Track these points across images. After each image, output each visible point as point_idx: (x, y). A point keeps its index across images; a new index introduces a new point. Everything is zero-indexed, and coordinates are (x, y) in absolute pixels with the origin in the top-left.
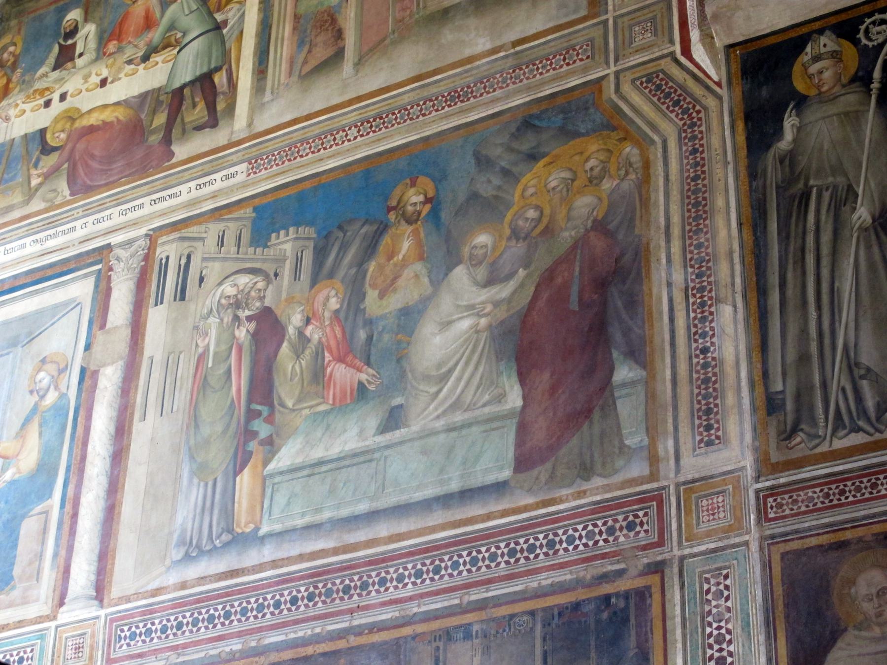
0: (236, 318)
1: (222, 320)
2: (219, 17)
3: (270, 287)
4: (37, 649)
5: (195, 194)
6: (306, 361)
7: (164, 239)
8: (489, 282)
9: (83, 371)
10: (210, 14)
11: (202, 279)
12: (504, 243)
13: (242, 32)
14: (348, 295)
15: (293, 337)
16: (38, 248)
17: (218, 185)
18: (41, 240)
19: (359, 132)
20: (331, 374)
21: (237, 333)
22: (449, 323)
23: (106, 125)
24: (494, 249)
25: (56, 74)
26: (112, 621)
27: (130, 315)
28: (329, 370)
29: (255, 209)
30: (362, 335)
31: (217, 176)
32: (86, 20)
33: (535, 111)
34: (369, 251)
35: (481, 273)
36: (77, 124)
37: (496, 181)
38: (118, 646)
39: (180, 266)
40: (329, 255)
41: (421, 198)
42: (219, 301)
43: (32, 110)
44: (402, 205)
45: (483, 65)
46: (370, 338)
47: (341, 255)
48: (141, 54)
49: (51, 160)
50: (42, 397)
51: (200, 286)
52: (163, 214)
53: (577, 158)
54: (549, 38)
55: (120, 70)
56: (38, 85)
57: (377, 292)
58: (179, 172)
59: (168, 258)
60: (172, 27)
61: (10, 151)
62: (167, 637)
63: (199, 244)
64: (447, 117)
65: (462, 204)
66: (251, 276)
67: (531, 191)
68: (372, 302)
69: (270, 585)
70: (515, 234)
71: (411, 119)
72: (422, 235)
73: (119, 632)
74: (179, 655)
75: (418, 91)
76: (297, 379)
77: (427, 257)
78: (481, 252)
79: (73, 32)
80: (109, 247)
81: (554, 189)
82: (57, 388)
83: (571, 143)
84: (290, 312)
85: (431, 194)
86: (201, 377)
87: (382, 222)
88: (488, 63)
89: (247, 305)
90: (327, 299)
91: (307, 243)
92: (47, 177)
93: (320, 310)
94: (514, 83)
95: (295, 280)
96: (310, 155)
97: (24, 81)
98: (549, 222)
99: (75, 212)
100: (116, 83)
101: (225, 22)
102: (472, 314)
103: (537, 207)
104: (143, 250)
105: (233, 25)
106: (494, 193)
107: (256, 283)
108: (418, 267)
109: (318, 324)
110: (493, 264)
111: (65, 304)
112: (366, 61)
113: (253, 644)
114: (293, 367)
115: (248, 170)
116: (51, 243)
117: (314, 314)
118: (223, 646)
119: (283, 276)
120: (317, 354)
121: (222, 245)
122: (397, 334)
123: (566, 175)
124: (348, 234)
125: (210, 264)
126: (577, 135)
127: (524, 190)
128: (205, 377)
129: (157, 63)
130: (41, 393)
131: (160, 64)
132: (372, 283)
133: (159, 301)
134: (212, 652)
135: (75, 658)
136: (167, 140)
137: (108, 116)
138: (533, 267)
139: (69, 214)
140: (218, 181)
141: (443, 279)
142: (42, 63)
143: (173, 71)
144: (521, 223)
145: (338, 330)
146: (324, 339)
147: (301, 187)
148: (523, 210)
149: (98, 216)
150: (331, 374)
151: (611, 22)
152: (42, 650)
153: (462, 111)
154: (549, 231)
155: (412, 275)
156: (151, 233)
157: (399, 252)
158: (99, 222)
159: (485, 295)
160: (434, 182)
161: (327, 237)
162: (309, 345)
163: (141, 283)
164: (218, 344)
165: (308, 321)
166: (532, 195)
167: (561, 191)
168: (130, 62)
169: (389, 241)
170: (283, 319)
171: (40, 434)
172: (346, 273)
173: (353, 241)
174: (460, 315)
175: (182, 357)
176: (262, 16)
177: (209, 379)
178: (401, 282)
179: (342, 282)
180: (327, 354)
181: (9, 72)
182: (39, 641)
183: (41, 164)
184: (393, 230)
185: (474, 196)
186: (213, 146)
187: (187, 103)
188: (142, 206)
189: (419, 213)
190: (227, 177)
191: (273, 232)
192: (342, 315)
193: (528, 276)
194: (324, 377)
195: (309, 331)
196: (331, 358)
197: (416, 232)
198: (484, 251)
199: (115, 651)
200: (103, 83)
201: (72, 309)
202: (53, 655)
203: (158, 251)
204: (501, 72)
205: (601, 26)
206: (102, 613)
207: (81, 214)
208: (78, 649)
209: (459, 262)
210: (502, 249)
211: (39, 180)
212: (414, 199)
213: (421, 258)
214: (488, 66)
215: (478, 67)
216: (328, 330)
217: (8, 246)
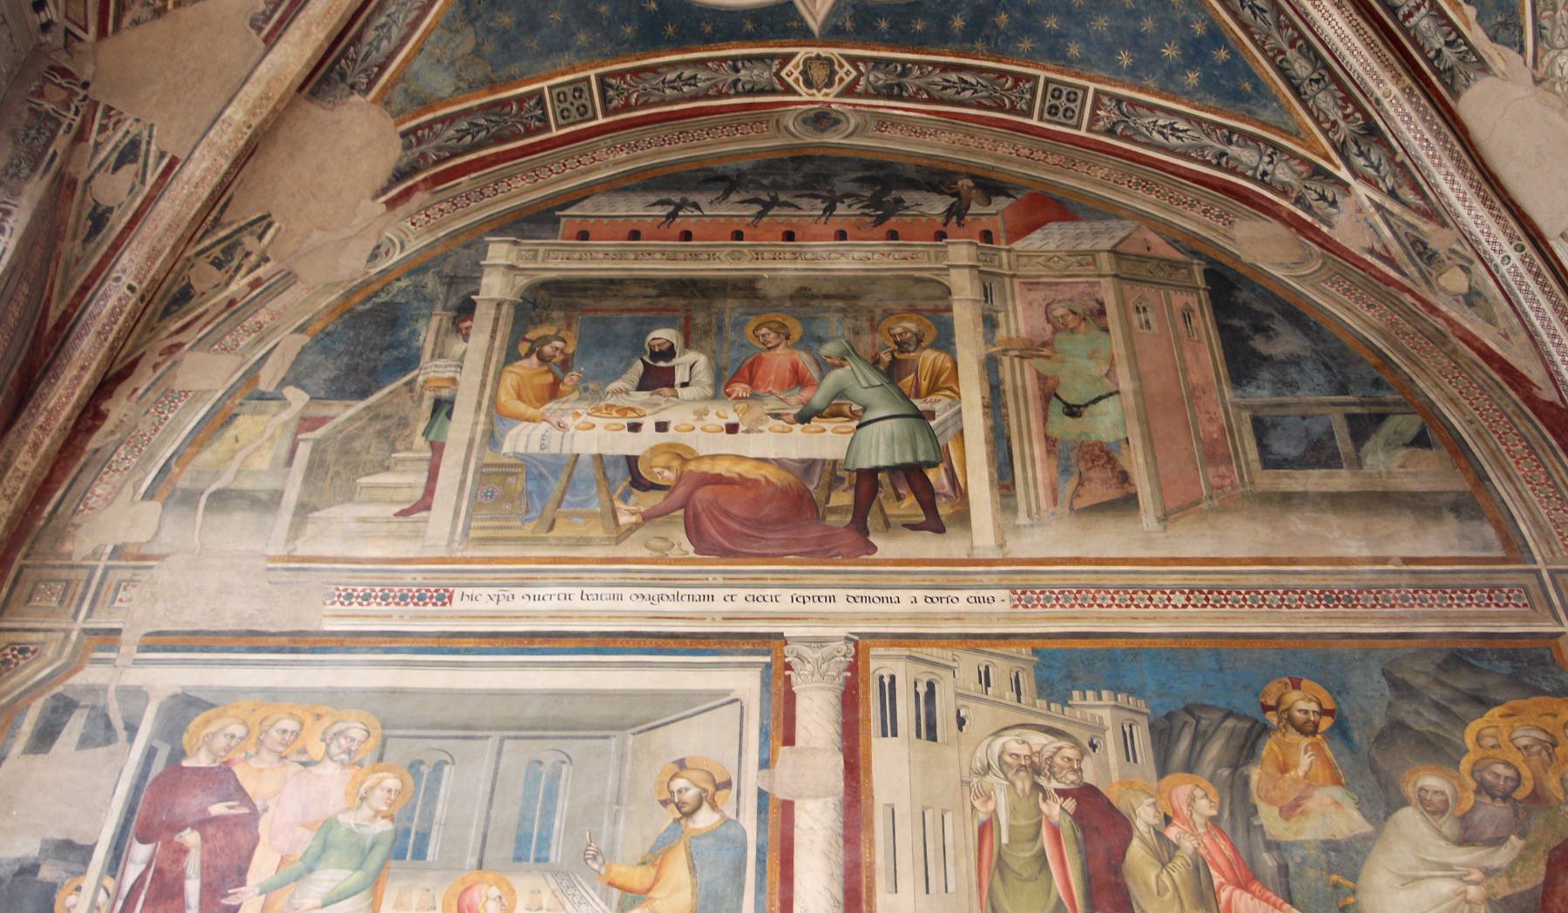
0: (1037, 787)
1: (1013, 784)
2: (921, 405)
3: (1087, 759)
5: (922, 606)
6: (1180, 873)
7: (881, 651)
8: (1466, 839)
9: (762, 795)
10: (906, 398)
11: (961, 722)
12: (1472, 796)
13: (961, 432)
14: (1227, 802)
15: (1147, 836)
16: (645, 606)
17: (962, 606)
18: (651, 598)
19: (1188, 599)
20: (1229, 902)
21: (1044, 807)
22: (1416, 879)
23: (742, 482)
24: (1457, 800)
25: (644, 396)
27: (838, 739)
28: (1223, 896)
29: (1035, 652)
30: (1268, 861)
31: (963, 594)
32: (687, 346)
33: (1464, 645)
34: (1245, 752)
35: (1448, 825)
36: (692, 466)
37: (1434, 718)
39: (917, 694)
40: (1178, 740)
41: (1313, 706)
42: (1000, 757)
43: (606, 427)
44: (1283, 707)
45: (1365, 572)
46: (1283, 869)
47: (1198, 746)
48: (796, 411)
49: (653, 500)
50: (689, 815)
51: (961, 730)
52: (868, 618)
53: (1549, 719)
54: (1457, 567)
55: (759, 421)
56: (611, 400)
57: (1276, 810)
58: (891, 573)
59: (893, 678)
60: (841, 393)
61: (573, 468)
63: (948, 674)
64: (1325, 617)
65: (1382, 730)
66: (1050, 738)
67: (1489, 742)
68: (1269, 818)
70: (1483, 788)
71: (1270, 606)
72: (1330, 754)
75: (1273, 576)
76: (1169, 895)
77: (1347, 784)
78: (1437, 798)
79: (669, 353)
80: (780, 636)
81: (1526, 747)
82: (714, 807)
83: (1535, 699)
84: (1132, 800)
85: (1328, 705)
86: (991, 852)
87: (1257, 721)
88: (1373, 572)
89: (1053, 774)
90: (1193, 799)
91: (1137, 717)
92: (648, 518)
93: (1185, 811)
94: (1420, 605)
95: (1128, 760)
96: (1115, 608)
97: (586, 389)
98: (1535, 784)
99: (711, 577)
100: (752, 436)
101: (932, 415)
102: (1452, 877)
103: (1508, 764)
104: (845, 656)
105: (945, 421)
106: (1432, 729)
107: (1060, 748)
108: (1337, 792)
109: (1186, 828)
110: (1463, 818)
111: (714, 694)
112: (1176, 520)
114: (1157, 877)
115: (1012, 600)
116: (668, 606)
117: (1174, 812)
119: (1105, 746)
120: (1197, 869)
121: (988, 684)
122: (1330, 872)
123: (1543, 736)
124: (1204, 722)
125: (972, 704)
126: (1538, 692)
127: (1478, 739)
128: (999, 853)
129: (824, 430)
130: (686, 809)
131: (829, 433)
132: (1262, 795)
133: (890, 728)
136: (860, 525)
137: (745, 469)
138: (1532, 838)
139: (704, 576)
140: (962, 601)
141: (1386, 819)
142: (617, 376)
143: (854, 447)
144: (1488, 777)
145: (1223, 844)
146: (1203, 851)
147: (1109, 643)
148: (1487, 762)
149: (757, 592)
150: (1229, 902)
151: (1545, 575)
153: (1344, 618)
154: (1537, 797)
155: (1328, 800)
156: (856, 638)
157: (1296, 766)
158: (756, 599)
159: (1461, 856)
160: (1330, 692)
161: (1169, 716)
162: (1178, 853)
163: (850, 700)
164: (1013, 812)
165: (1168, 820)
166: (1493, 747)
167: (1539, 753)
168: (777, 416)
169: (1275, 748)
170: (1121, 805)
171: (692, 869)
172: (1214, 773)
173: (1214, 733)
174: (1432, 873)
175: (948, 817)
176: (990, 422)
177: (1008, 859)
178: (1310, 804)
179: (1211, 779)
180: (1213, 872)
181: (557, 370)
183: (633, 499)
184: (1279, 735)
185: (1397, 727)
186: (944, 555)
187: (885, 491)
188: (832, 599)
189: (1316, 725)
190: (977, 600)
191: (1074, 688)
192: (1225, 826)
193: (1527, 848)
194: (1217, 902)
195: (1172, 833)
196: (1223, 880)
197: (1317, 747)
198: (1443, 798)
200: (732, 429)
201: (722, 705)
203: (873, 665)
204: (1398, 588)
205: (1559, 577)
207: (720, 581)
209: (1404, 803)
210: (1471, 803)
211: (634, 519)
212: (1302, 705)
213: (1337, 782)
214: (1374, 576)
215: (1357, 573)
216: (1206, 840)
217: (587, 590)
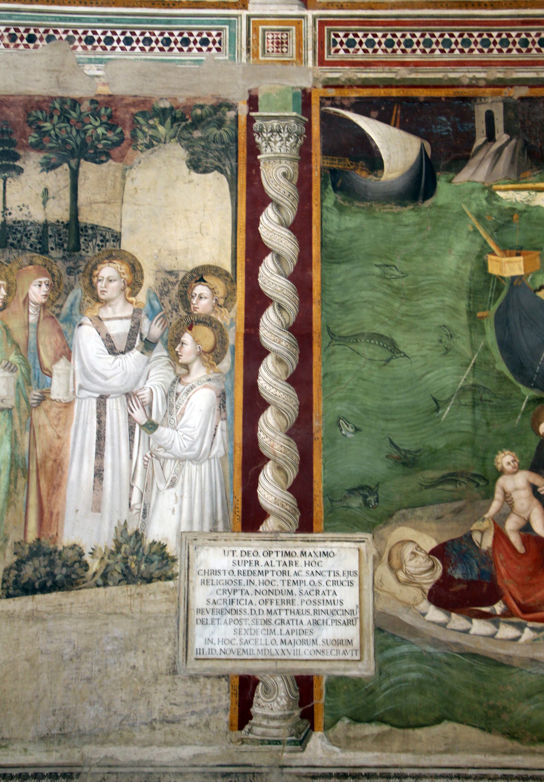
4: (226, 35)
26: (322, 24)
38: (333, 50)
62: (394, 51)
69: (512, 23)
73: (333, 37)
74: (411, 72)
113: (500, 75)
118: (465, 72)
134: (452, 75)
135: (278, 52)
152: (233, 36)
182: (227, 27)
199: (329, 53)
202: (248, 43)
206: (310, 13)
208: (280, 44)
